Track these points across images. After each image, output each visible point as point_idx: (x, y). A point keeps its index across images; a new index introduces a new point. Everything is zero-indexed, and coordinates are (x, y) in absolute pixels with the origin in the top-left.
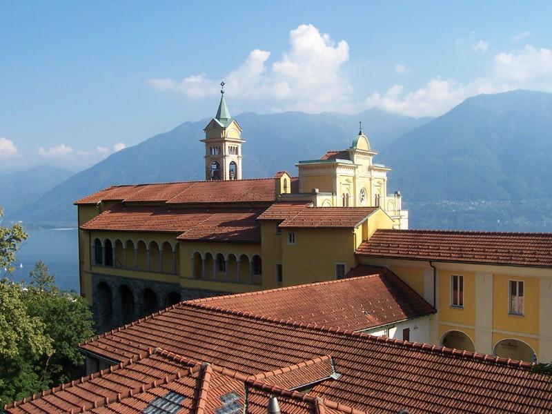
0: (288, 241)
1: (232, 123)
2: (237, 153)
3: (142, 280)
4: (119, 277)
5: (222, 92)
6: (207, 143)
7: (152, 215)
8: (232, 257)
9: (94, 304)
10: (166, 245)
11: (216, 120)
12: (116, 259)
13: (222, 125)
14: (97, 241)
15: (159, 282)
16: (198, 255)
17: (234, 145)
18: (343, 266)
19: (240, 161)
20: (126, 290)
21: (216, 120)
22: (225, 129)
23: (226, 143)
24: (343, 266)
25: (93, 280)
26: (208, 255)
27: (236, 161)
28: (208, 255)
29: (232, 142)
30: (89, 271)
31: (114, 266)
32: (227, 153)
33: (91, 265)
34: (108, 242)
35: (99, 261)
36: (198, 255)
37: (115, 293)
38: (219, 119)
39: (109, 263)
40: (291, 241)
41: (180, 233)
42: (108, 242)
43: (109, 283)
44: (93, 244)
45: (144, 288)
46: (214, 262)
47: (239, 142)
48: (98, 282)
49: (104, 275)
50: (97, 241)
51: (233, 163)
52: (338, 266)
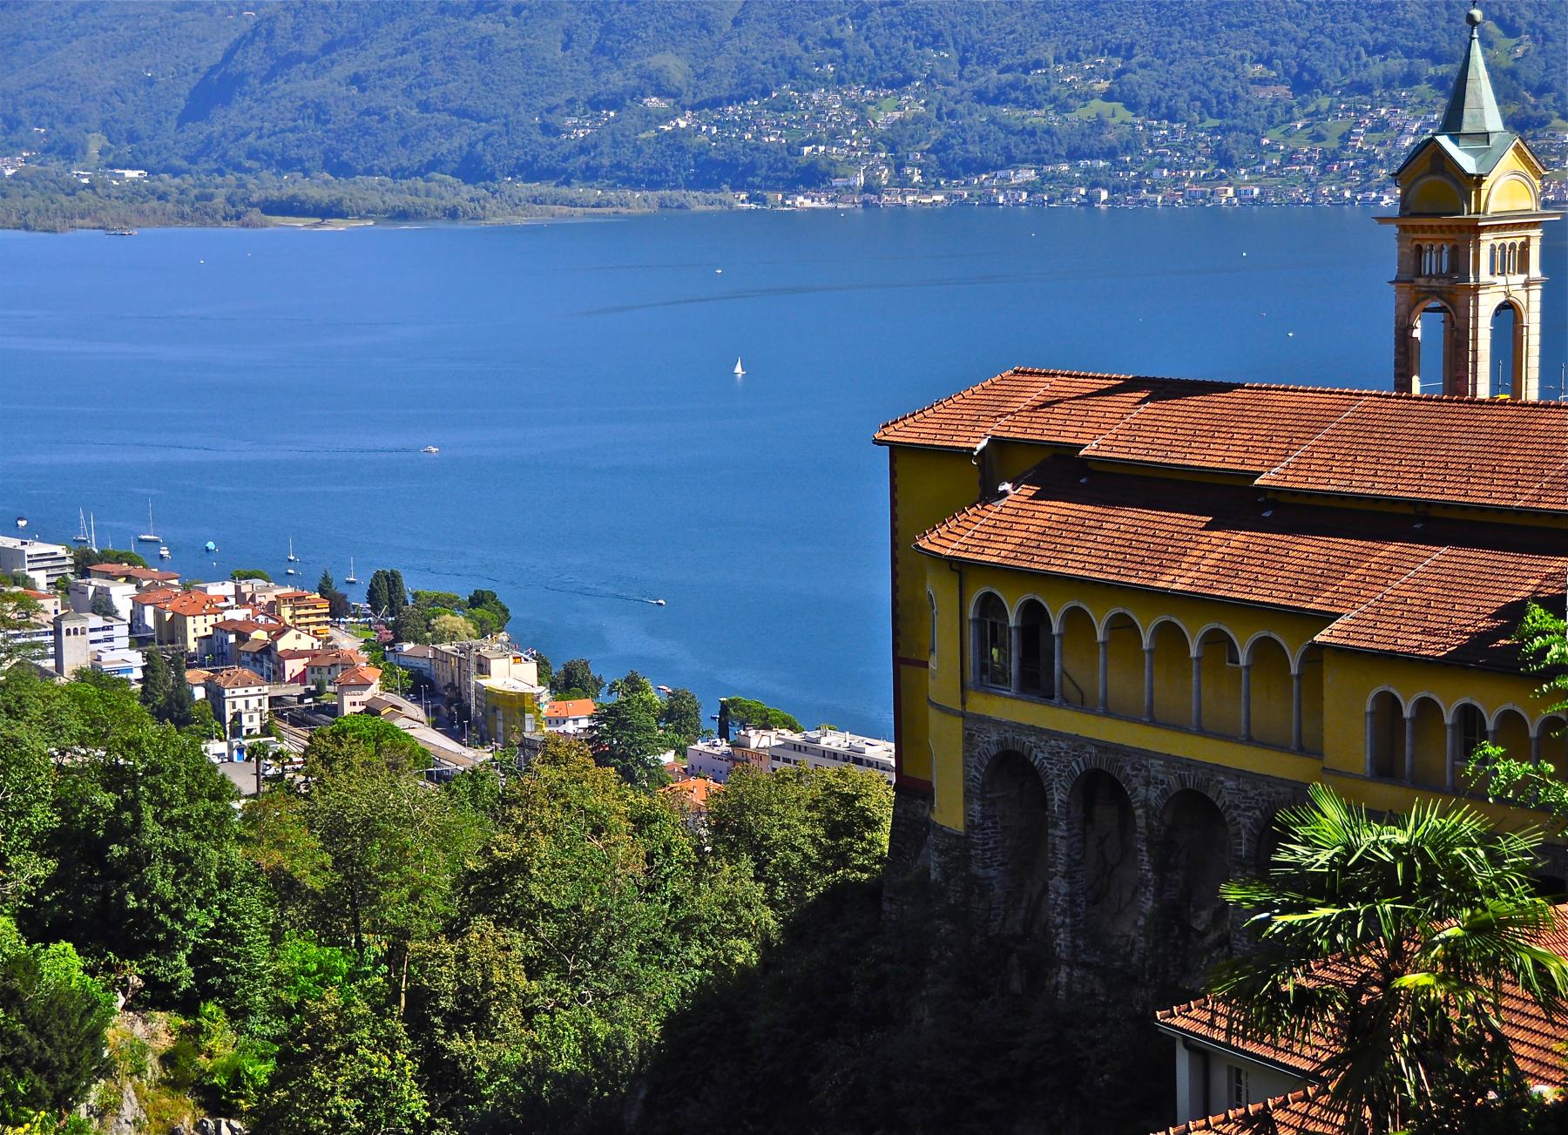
1: (1510, 153)
2: (1524, 267)
3: (1170, 760)
4: (1079, 743)
6: (1403, 228)
7: (1209, 527)
9: (970, 826)
10: (1266, 650)
11: (1444, 140)
12: (1063, 670)
13: (1468, 164)
14: (990, 605)
15: (1238, 774)
16: (1388, 704)
17: (1517, 238)
19: (1536, 294)
21: (1444, 140)
22: (1479, 180)
23: (1483, 236)
25: (969, 739)
26: (1427, 707)
27: (1519, 296)
28: (1427, 707)
29: (1514, 227)
30: (959, 708)
31: (1056, 700)
32: (1485, 276)
33: (963, 687)
34: (1034, 614)
35: (990, 677)
36: (1388, 704)
37: (1058, 797)
38: (1455, 139)
39: (1036, 681)
41: (1327, 618)
42: (1034, 614)
43: (1038, 757)
44: (971, 613)
45: (1176, 787)
46: (1449, 731)
47: (1534, 225)
48: (994, 751)
49: (1018, 727)
50: (990, 605)
51: (1508, 311)
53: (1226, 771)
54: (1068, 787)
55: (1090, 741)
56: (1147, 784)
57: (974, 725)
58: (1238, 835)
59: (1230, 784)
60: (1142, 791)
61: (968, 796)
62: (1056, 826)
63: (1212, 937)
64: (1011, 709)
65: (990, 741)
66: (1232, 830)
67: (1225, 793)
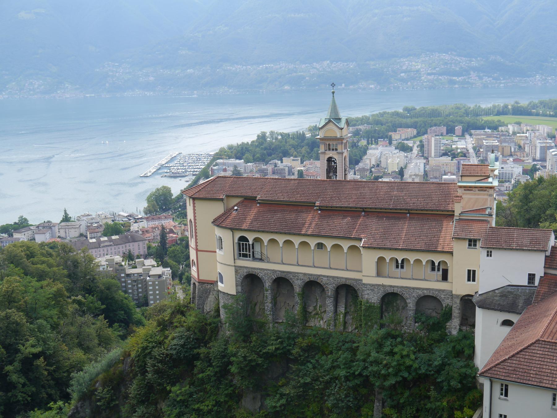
0: (486, 255)
3: (305, 274)
4: (274, 271)
5: (333, 93)
8: (418, 261)
18: (534, 275)
20: (282, 282)
24: (534, 275)
25: (236, 272)
40: (488, 256)
43: (260, 275)
44: (236, 241)
48: (245, 274)
49: (254, 268)
50: (243, 239)
52: (529, 275)
53: (324, 276)
54: (271, 282)
55: (278, 271)
56: (297, 279)
57: (237, 269)
58: (328, 290)
59: (326, 279)
60: (296, 282)
61: (237, 286)
62: (267, 291)
63: (314, 313)
64: (248, 264)
65: (245, 272)
66: (326, 289)
67: (324, 281)
